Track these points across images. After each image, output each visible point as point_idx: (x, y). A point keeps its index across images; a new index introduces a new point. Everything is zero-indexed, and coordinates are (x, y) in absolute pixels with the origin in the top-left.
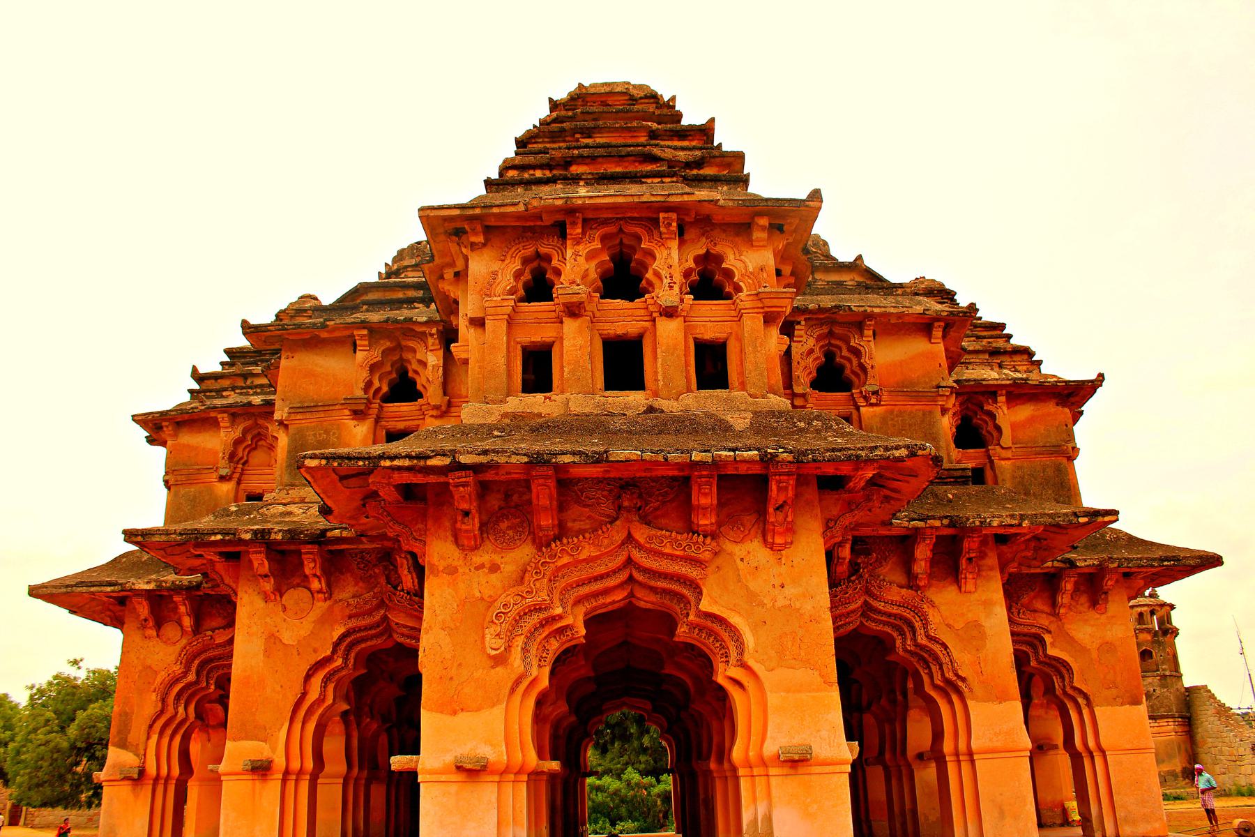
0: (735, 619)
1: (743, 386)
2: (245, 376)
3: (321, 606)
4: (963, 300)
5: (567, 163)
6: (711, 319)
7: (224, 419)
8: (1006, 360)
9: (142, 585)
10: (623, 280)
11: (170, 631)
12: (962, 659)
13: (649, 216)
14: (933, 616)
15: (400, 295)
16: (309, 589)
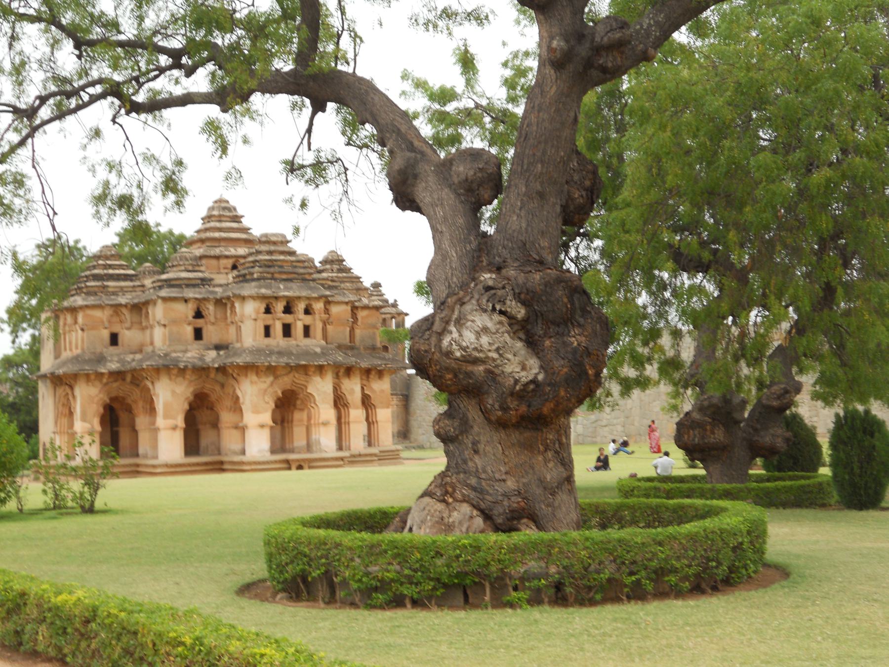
0: (314, 394)
1: (315, 338)
2: (105, 287)
3: (186, 382)
4: (348, 263)
5: (272, 274)
6: (308, 320)
7: (108, 308)
8: (361, 292)
9: (103, 371)
10: (288, 310)
11: (97, 383)
12: (349, 398)
13: (299, 298)
14: (343, 387)
15: (193, 282)
16: (184, 378)
